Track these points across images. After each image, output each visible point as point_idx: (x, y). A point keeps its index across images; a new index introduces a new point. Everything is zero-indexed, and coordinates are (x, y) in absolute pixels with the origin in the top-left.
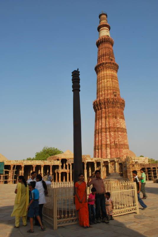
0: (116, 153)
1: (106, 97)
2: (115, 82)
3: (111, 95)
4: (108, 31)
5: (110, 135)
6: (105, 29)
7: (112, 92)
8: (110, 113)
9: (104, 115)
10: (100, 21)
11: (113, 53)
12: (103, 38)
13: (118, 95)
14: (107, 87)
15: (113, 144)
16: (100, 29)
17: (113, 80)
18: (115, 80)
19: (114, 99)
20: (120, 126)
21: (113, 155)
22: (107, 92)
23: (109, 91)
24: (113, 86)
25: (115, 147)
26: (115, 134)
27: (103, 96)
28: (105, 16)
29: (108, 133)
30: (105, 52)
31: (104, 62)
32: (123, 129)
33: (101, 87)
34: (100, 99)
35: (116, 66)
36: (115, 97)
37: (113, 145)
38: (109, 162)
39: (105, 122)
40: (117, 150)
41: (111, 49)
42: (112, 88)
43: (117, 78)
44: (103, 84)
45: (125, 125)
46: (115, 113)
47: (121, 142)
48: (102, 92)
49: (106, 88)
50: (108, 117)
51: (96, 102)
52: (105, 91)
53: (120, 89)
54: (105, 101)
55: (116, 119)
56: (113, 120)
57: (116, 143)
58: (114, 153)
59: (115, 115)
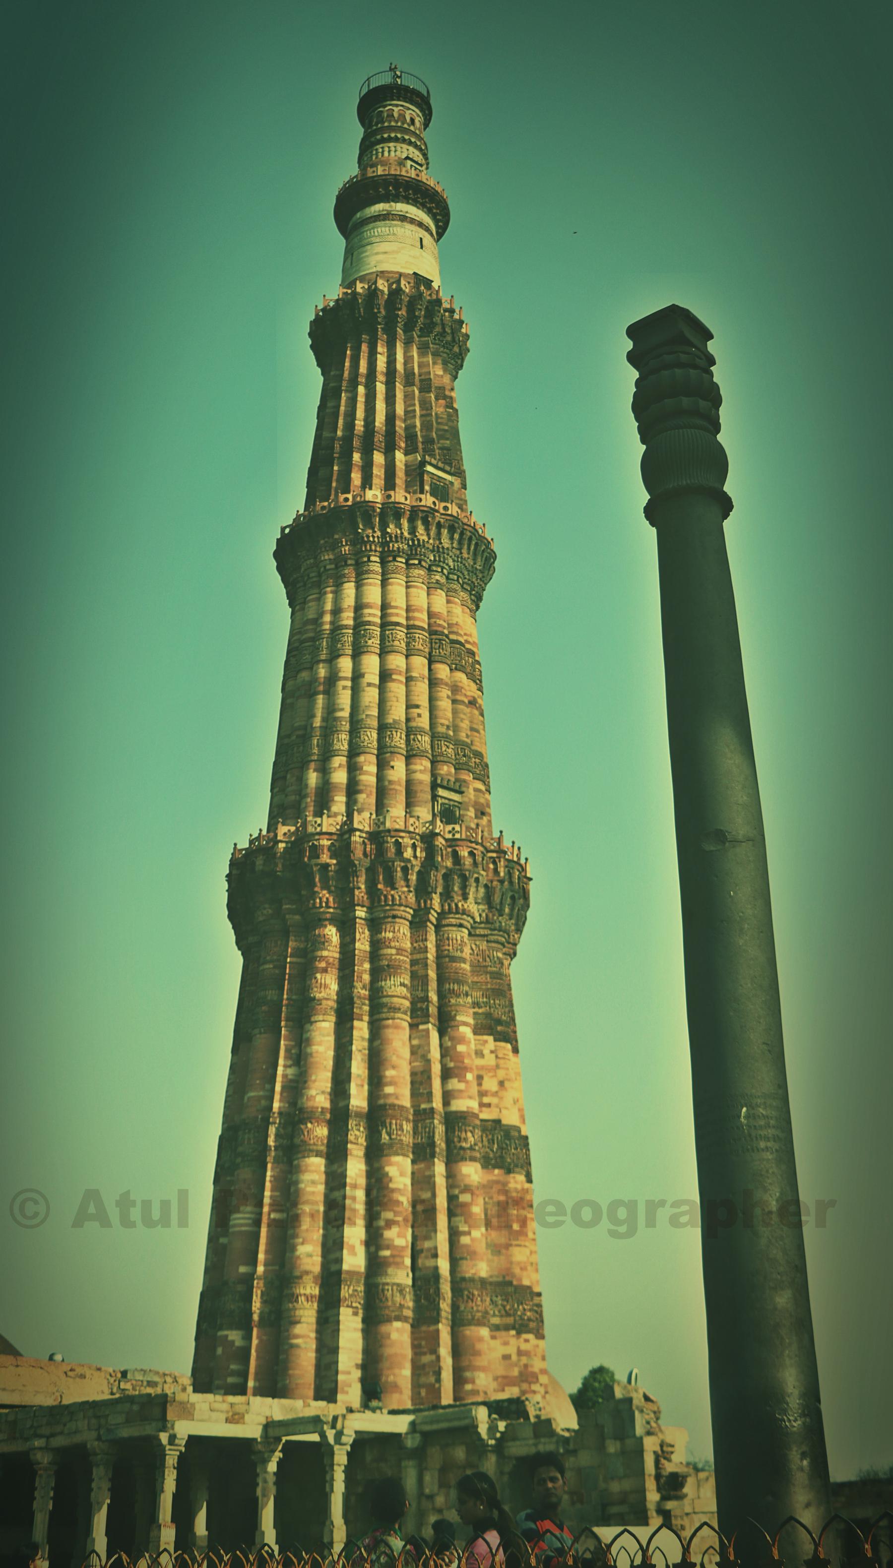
0: (418, 1369)
1: (363, 821)
2: (455, 689)
3: (409, 805)
4: (428, 240)
5: (377, 1184)
6: (403, 218)
7: (426, 778)
8: (392, 969)
9: (328, 986)
10: (367, 146)
11: (455, 434)
12: (382, 285)
13: (471, 813)
14: (383, 728)
15: (402, 1275)
16: (358, 215)
17: (443, 671)
18: (461, 677)
19: (440, 842)
20: (474, 1105)
21: (396, 1387)
22: (373, 769)
23: (398, 771)
24: (441, 729)
25: (418, 1309)
26: (422, 1181)
27: (339, 803)
28: (412, 112)
29: (355, 1168)
30: (391, 418)
31: (370, 495)
32: (499, 1136)
33: (317, 722)
34: (310, 829)
35: (475, 554)
36: (439, 827)
37: (401, 1289)
38: (410, 1443)
39: (331, 1053)
40: (435, 1337)
41: (441, 394)
42: (425, 741)
43: (472, 653)
44: (344, 699)
45: (516, 1101)
46: (432, 974)
47: (473, 1254)
48: (324, 770)
49: (371, 737)
50: (366, 1008)
51: (259, 862)
52: (362, 758)
53: (490, 759)
54: (358, 853)
55: (442, 1032)
56: (415, 1042)
57: (425, 1262)
58: (407, 1372)
59: (433, 997)
